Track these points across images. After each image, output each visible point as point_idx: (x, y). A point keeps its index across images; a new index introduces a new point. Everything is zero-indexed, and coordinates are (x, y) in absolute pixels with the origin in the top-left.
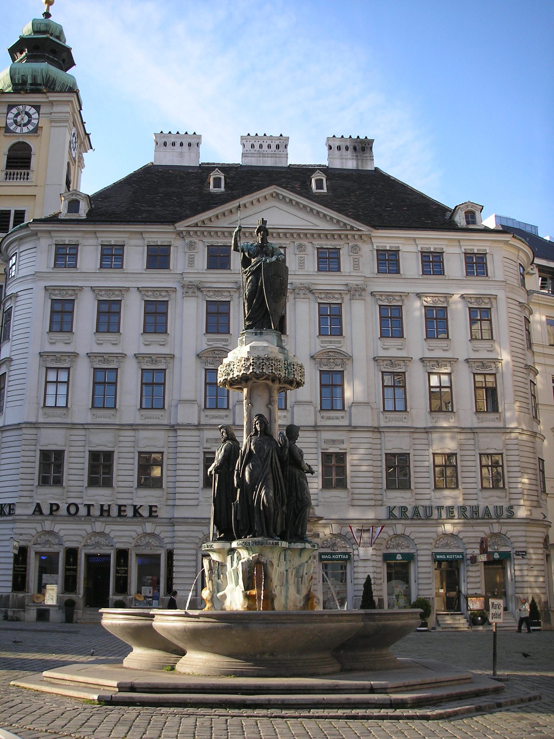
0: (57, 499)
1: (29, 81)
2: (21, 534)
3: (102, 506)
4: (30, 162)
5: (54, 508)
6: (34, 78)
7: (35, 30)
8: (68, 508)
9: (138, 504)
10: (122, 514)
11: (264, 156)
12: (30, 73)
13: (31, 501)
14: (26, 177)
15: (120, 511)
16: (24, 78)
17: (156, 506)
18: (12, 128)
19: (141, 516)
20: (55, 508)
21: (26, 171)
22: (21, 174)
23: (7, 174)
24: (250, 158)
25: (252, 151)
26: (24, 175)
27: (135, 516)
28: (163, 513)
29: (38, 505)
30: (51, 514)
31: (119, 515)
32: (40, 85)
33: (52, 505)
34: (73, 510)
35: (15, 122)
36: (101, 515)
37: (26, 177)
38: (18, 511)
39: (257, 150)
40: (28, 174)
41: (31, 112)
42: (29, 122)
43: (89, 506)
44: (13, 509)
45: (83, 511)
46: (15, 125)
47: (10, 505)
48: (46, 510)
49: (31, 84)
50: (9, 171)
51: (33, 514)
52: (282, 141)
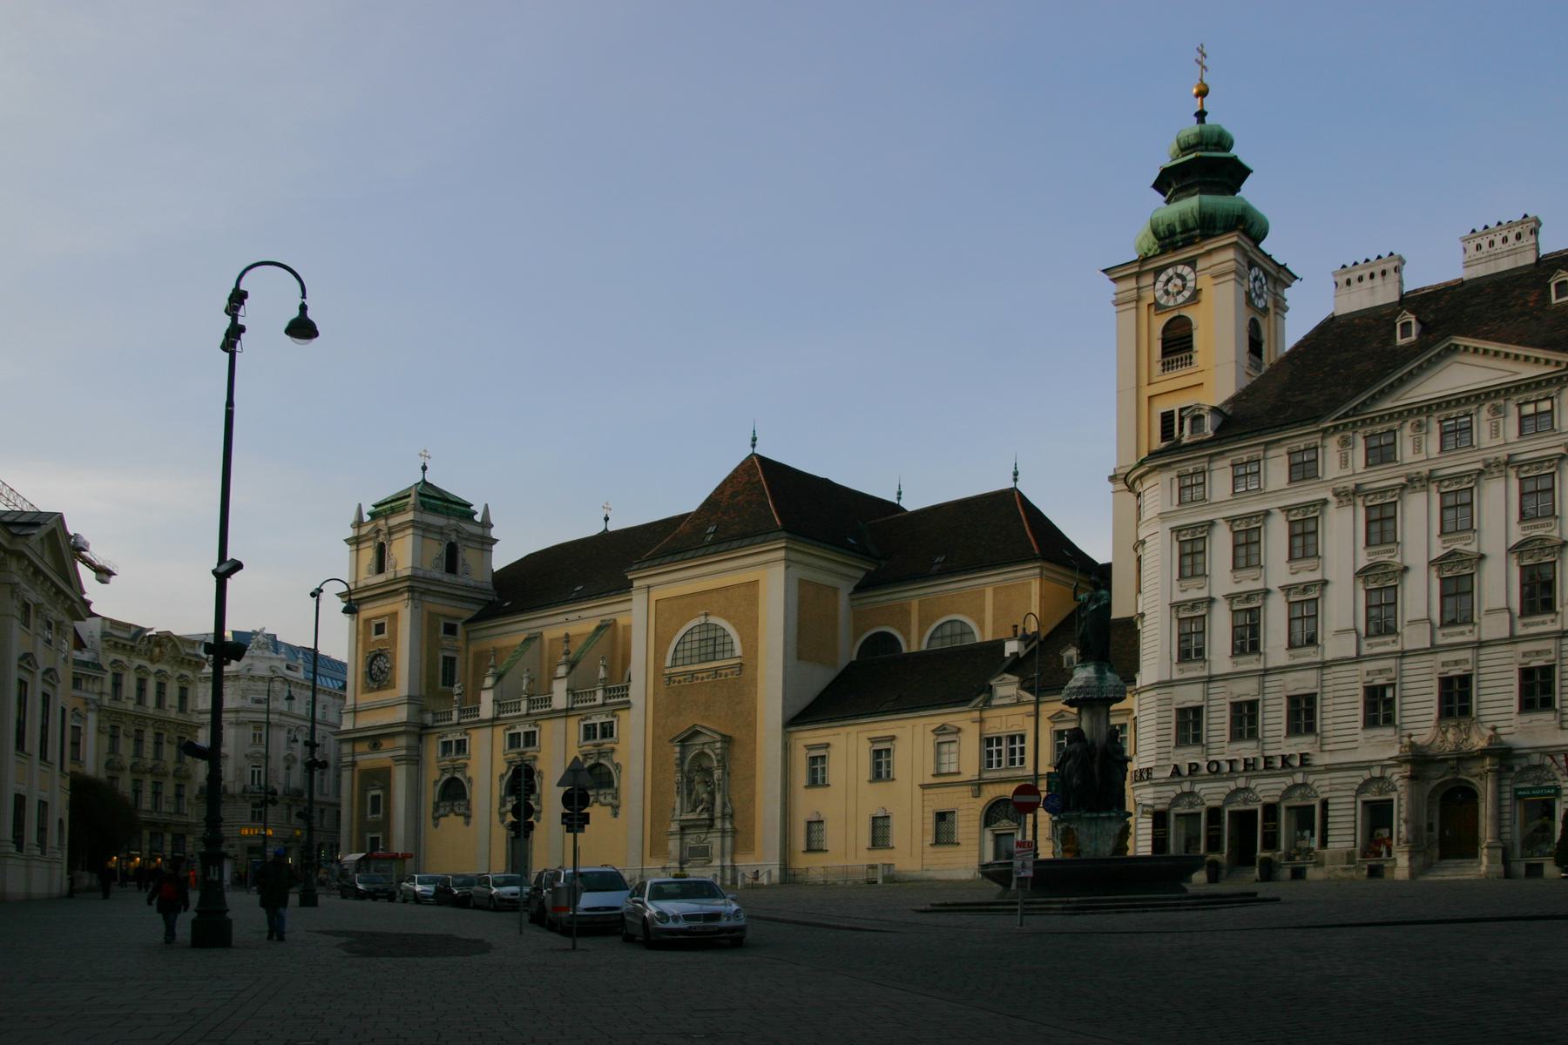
0: (1195, 758)
1: (1178, 230)
2: (1160, 798)
3: (1246, 760)
4: (1191, 341)
5: (1194, 768)
6: (1184, 223)
7: (1183, 146)
8: (1208, 767)
9: (1287, 753)
10: (1268, 765)
11: (1497, 256)
12: (1178, 219)
13: (1168, 763)
14: (1188, 361)
15: (1266, 763)
16: (1171, 227)
17: (1307, 754)
18: (1162, 302)
19: (1291, 766)
20: (1194, 767)
21: (1188, 354)
22: (1182, 360)
23: (1163, 364)
24: (1474, 267)
25: (1479, 254)
26: (1186, 359)
27: (1283, 766)
28: (1320, 760)
29: (1176, 766)
30: (1190, 774)
31: (1266, 768)
32: (1194, 229)
33: (1190, 765)
34: (1214, 768)
35: (1167, 293)
36: (1245, 770)
37: (1188, 361)
38: (1155, 775)
39: (1485, 251)
40: (1191, 357)
41: (1184, 273)
42: (1184, 286)
43: (1231, 762)
44: (1151, 774)
45: (1226, 768)
46: (1166, 297)
47: (1148, 769)
48: (1186, 771)
49: (1181, 233)
50: (1166, 360)
51: (1171, 776)
52: (1524, 226)
